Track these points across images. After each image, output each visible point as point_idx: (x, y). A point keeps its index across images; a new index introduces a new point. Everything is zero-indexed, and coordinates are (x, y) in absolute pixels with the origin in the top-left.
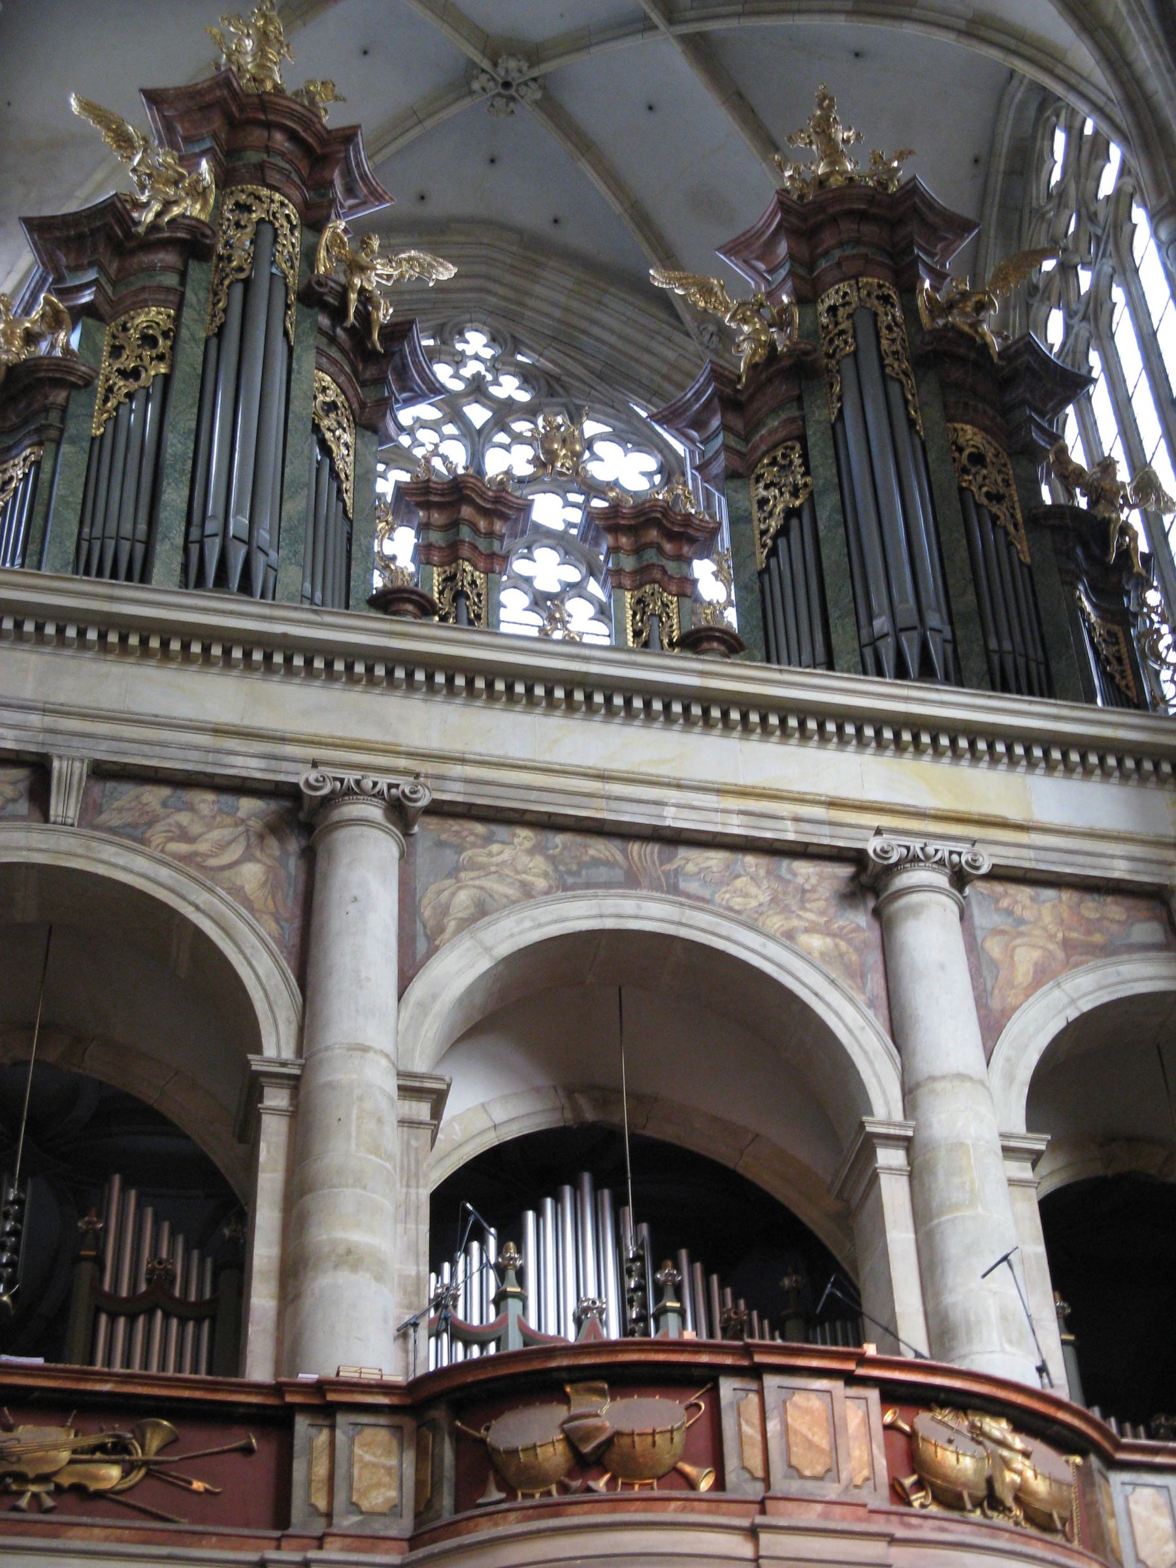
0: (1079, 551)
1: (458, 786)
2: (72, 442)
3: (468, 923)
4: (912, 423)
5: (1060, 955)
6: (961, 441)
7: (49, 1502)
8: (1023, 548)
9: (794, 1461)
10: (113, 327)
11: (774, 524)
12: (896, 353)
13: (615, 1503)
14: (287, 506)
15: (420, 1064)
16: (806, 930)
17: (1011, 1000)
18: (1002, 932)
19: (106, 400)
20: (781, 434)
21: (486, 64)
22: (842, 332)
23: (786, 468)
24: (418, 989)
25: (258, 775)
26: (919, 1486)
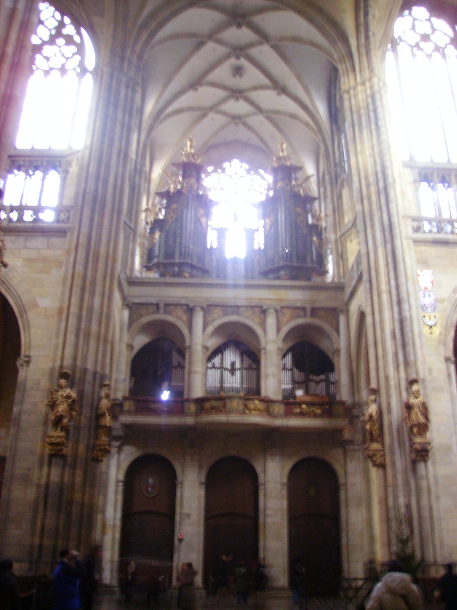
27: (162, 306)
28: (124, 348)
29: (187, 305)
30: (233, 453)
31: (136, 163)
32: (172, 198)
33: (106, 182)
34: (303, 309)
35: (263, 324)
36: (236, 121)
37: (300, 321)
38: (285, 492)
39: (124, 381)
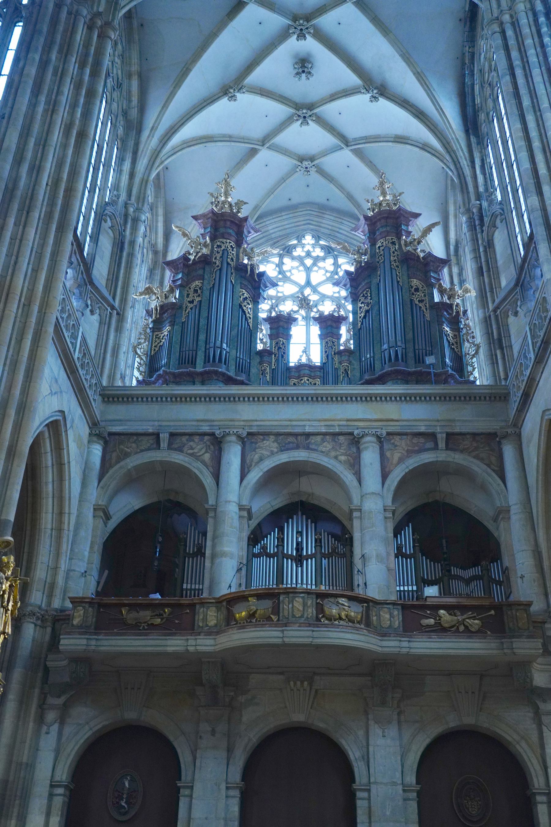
0: (445, 313)
1: (255, 428)
2: (177, 325)
3: (258, 463)
4: (398, 282)
5: (406, 454)
6: (412, 285)
7: (146, 627)
8: (428, 315)
9: (294, 613)
10: (187, 288)
11: (363, 315)
12: (395, 260)
13: (256, 626)
14: (232, 333)
15: (245, 502)
16: (341, 455)
17: (392, 468)
18: (391, 449)
19: (186, 311)
20: (365, 287)
21: (300, 164)
22: (381, 255)
23: (366, 298)
24: (245, 482)
25: (208, 431)
26: (323, 617)
27: (164, 437)
28: (89, 513)
29: (213, 434)
30: (299, 717)
31: (126, 205)
32: (190, 269)
33: (36, 169)
34: (432, 436)
35: (355, 465)
36: (306, 163)
37: (427, 457)
38: (413, 805)
39: (84, 574)
